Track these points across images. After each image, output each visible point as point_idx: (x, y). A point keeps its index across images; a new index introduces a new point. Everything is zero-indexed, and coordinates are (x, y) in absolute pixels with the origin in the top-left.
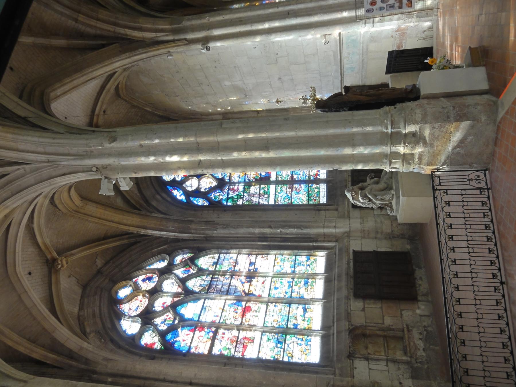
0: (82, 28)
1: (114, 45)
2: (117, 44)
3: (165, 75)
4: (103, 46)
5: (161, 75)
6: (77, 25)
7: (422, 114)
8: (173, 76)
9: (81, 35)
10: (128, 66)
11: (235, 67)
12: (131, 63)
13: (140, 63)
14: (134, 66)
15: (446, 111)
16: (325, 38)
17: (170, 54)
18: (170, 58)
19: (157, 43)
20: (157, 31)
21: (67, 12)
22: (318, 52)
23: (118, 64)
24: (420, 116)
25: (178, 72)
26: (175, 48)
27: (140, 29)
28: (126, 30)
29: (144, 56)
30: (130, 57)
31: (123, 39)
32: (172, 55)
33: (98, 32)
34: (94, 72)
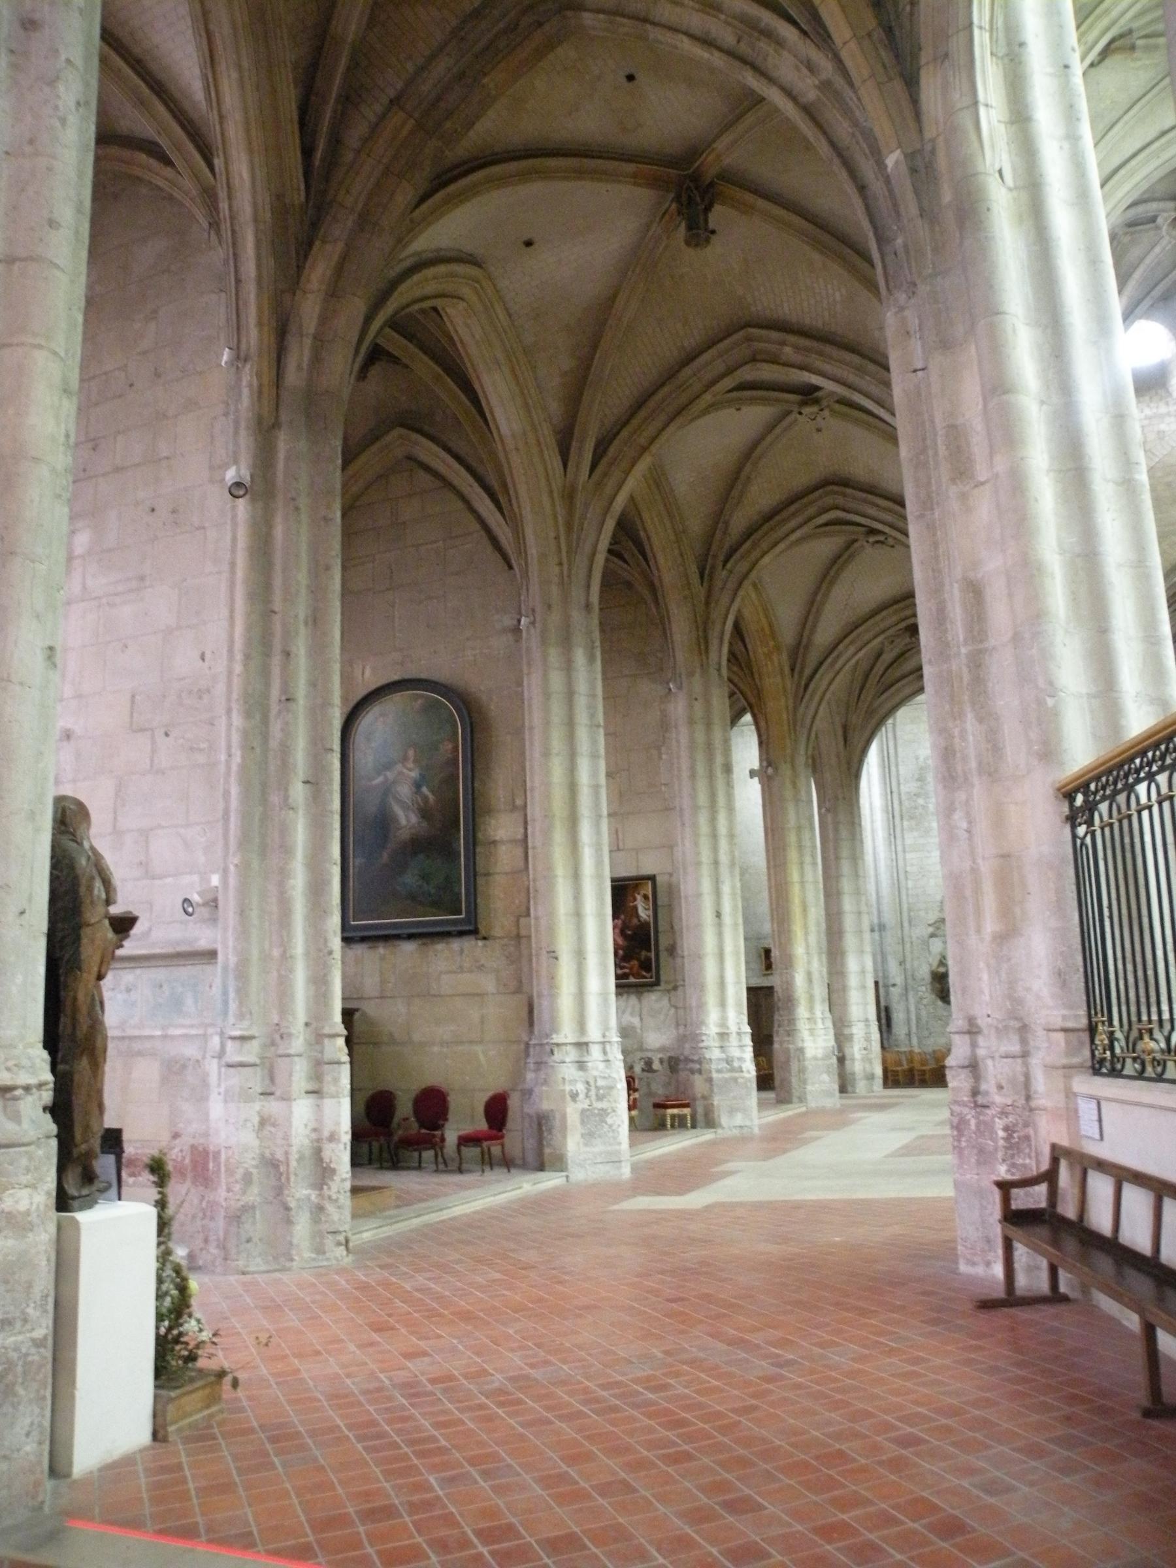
0: (370, 112)
1: (302, 187)
2: (303, 198)
3: (152, 326)
4: (307, 152)
5: (155, 311)
6: (385, 100)
7: (28, 1213)
8: (145, 353)
9: (350, 99)
10: (224, 206)
11: (142, 578)
12: (232, 218)
13: (218, 255)
14: (215, 225)
15: (30, 1311)
16: (205, 904)
17: (240, 357)
18: (226, 356)
19: (281, 329)
20: (320, 342)
21: (427, 87)
22: (153, 878)
23: (243, 173)
24: (23, 1206)
25: (157, 375)
26: (255, 382)
27: (333, 293)
28: (340, 246)
29: (249, 268)
30: (256, 220)
31: (315, 225)
32: (230, 363)
33: (349, 156)
34: (234, 75)
